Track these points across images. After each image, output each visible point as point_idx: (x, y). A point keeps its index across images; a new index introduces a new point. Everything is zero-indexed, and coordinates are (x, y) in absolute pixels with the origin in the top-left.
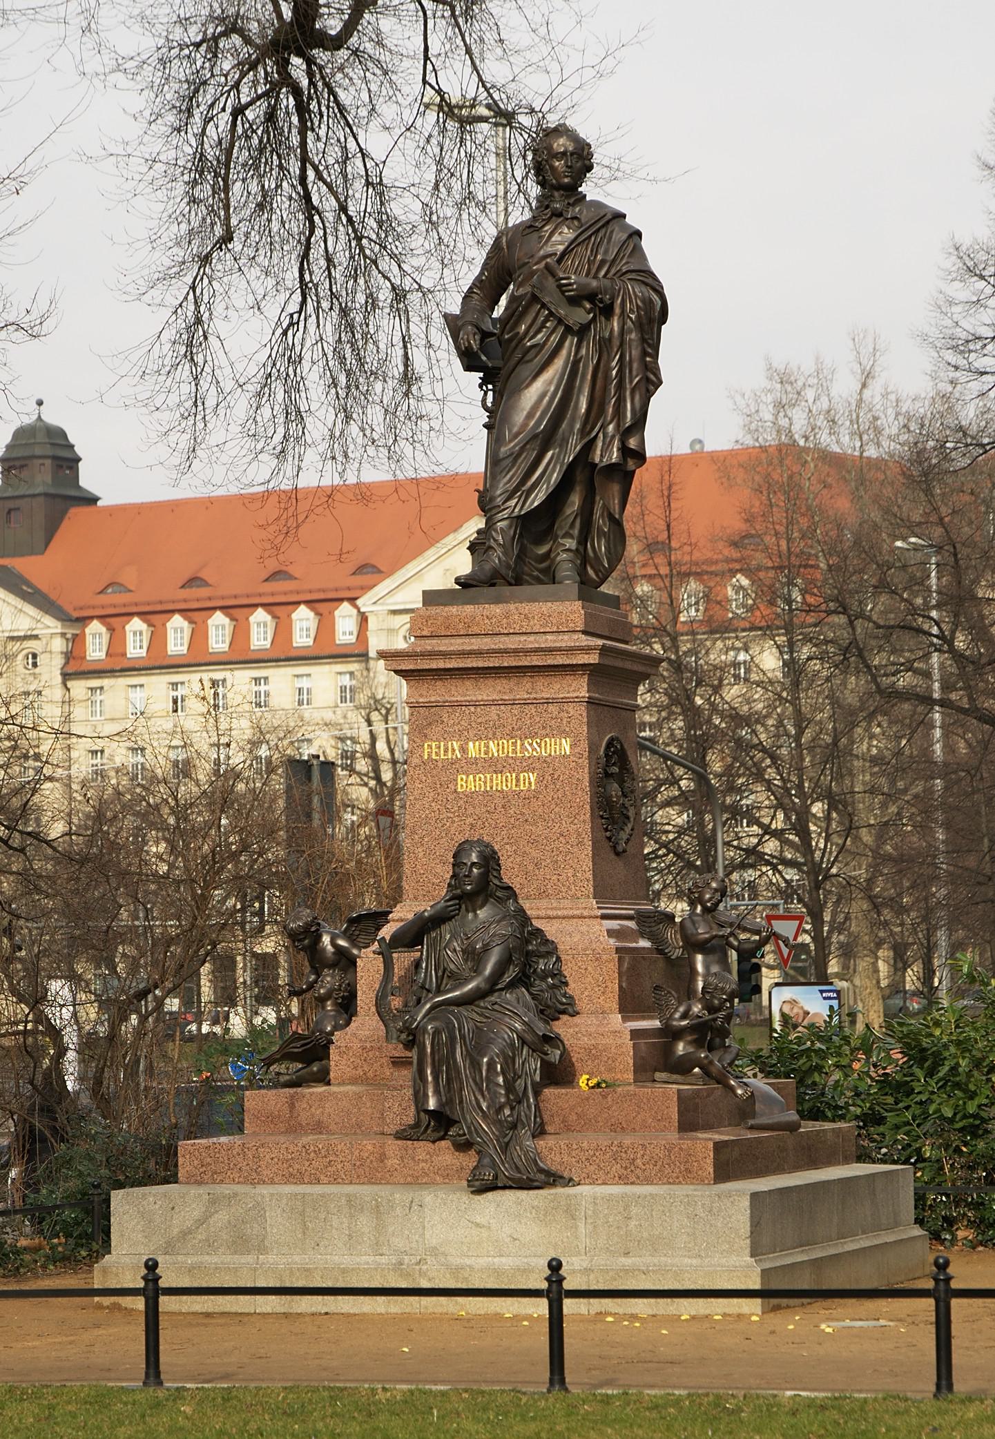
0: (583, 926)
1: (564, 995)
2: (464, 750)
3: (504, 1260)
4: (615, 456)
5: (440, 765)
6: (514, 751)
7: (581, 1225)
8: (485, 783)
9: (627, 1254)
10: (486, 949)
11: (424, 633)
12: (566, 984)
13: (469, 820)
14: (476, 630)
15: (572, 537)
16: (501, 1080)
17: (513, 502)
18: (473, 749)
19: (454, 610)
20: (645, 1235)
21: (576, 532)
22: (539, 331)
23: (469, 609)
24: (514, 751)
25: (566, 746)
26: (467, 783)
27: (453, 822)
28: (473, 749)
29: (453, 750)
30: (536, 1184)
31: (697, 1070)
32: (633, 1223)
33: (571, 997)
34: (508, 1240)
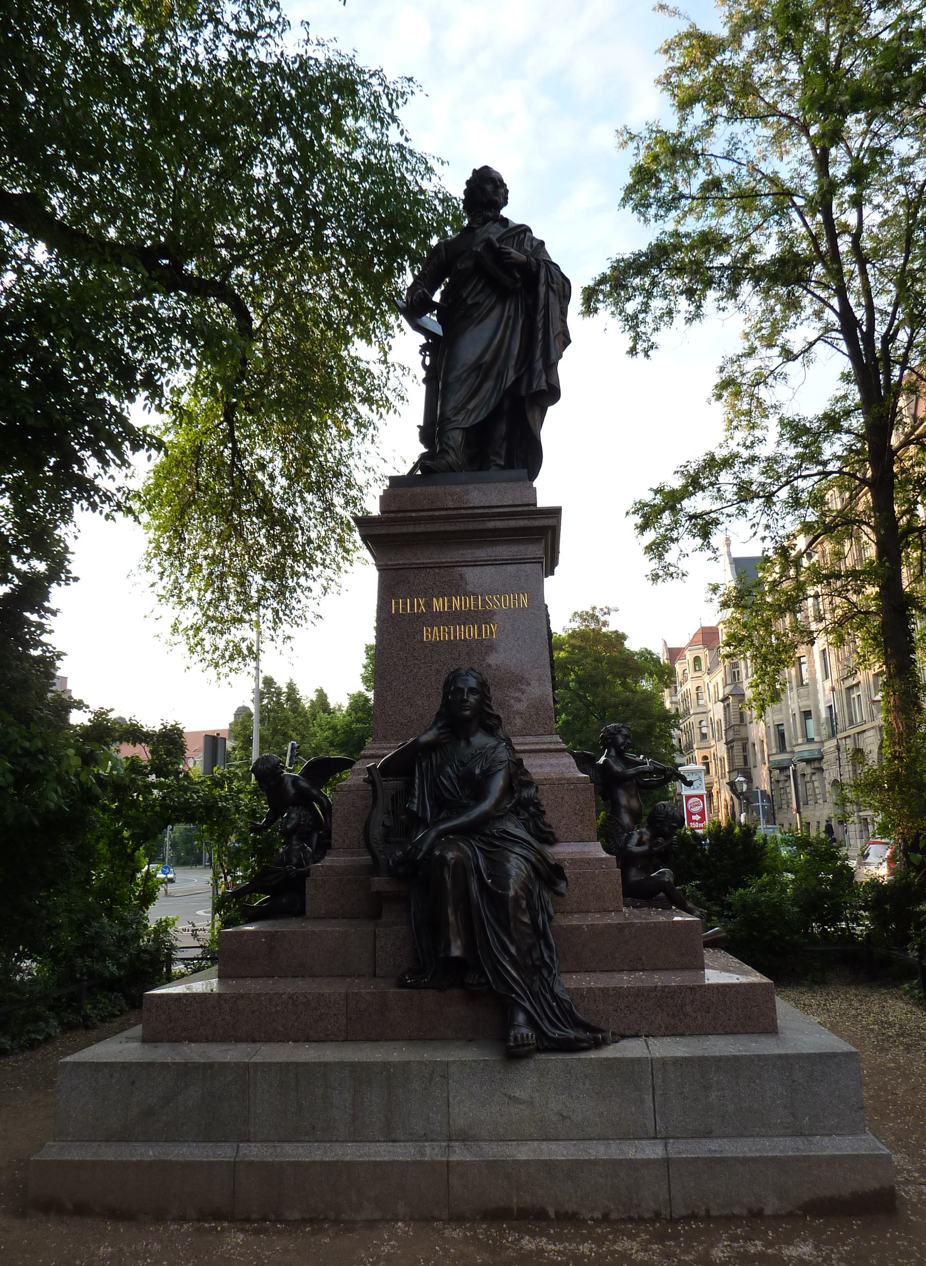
0: (553, 760)
1: (544, 823)
2: (429, 605)
3: (553, 1146)
4: (544, 386)
5: (407, 618)
6: (476, 606)
7: (648, 1098)
8: (449, 633)
9: (708, 1134)
10: (488, 775)
11: (393, 508)
12: (544, 812)
13: (435, 666)
14: (439, 505)
15: (499, 455)
16: (526, 919)
17: (460, 417)
18: (438, 604)
19: (418, 490)
20: (731, 1108)
21: (503, 453)
22: (477, 294)
23: (432, 489)
24: (476, 606)
25: (524, 600)
26: (434, 634)
27: (420, 668)
28: (438, 604)
29: (419, 605)
30: (585, 1045)
31: (662, 894)
32: (714, 1095)
33: (550, 826)
34: (555, 1119)
